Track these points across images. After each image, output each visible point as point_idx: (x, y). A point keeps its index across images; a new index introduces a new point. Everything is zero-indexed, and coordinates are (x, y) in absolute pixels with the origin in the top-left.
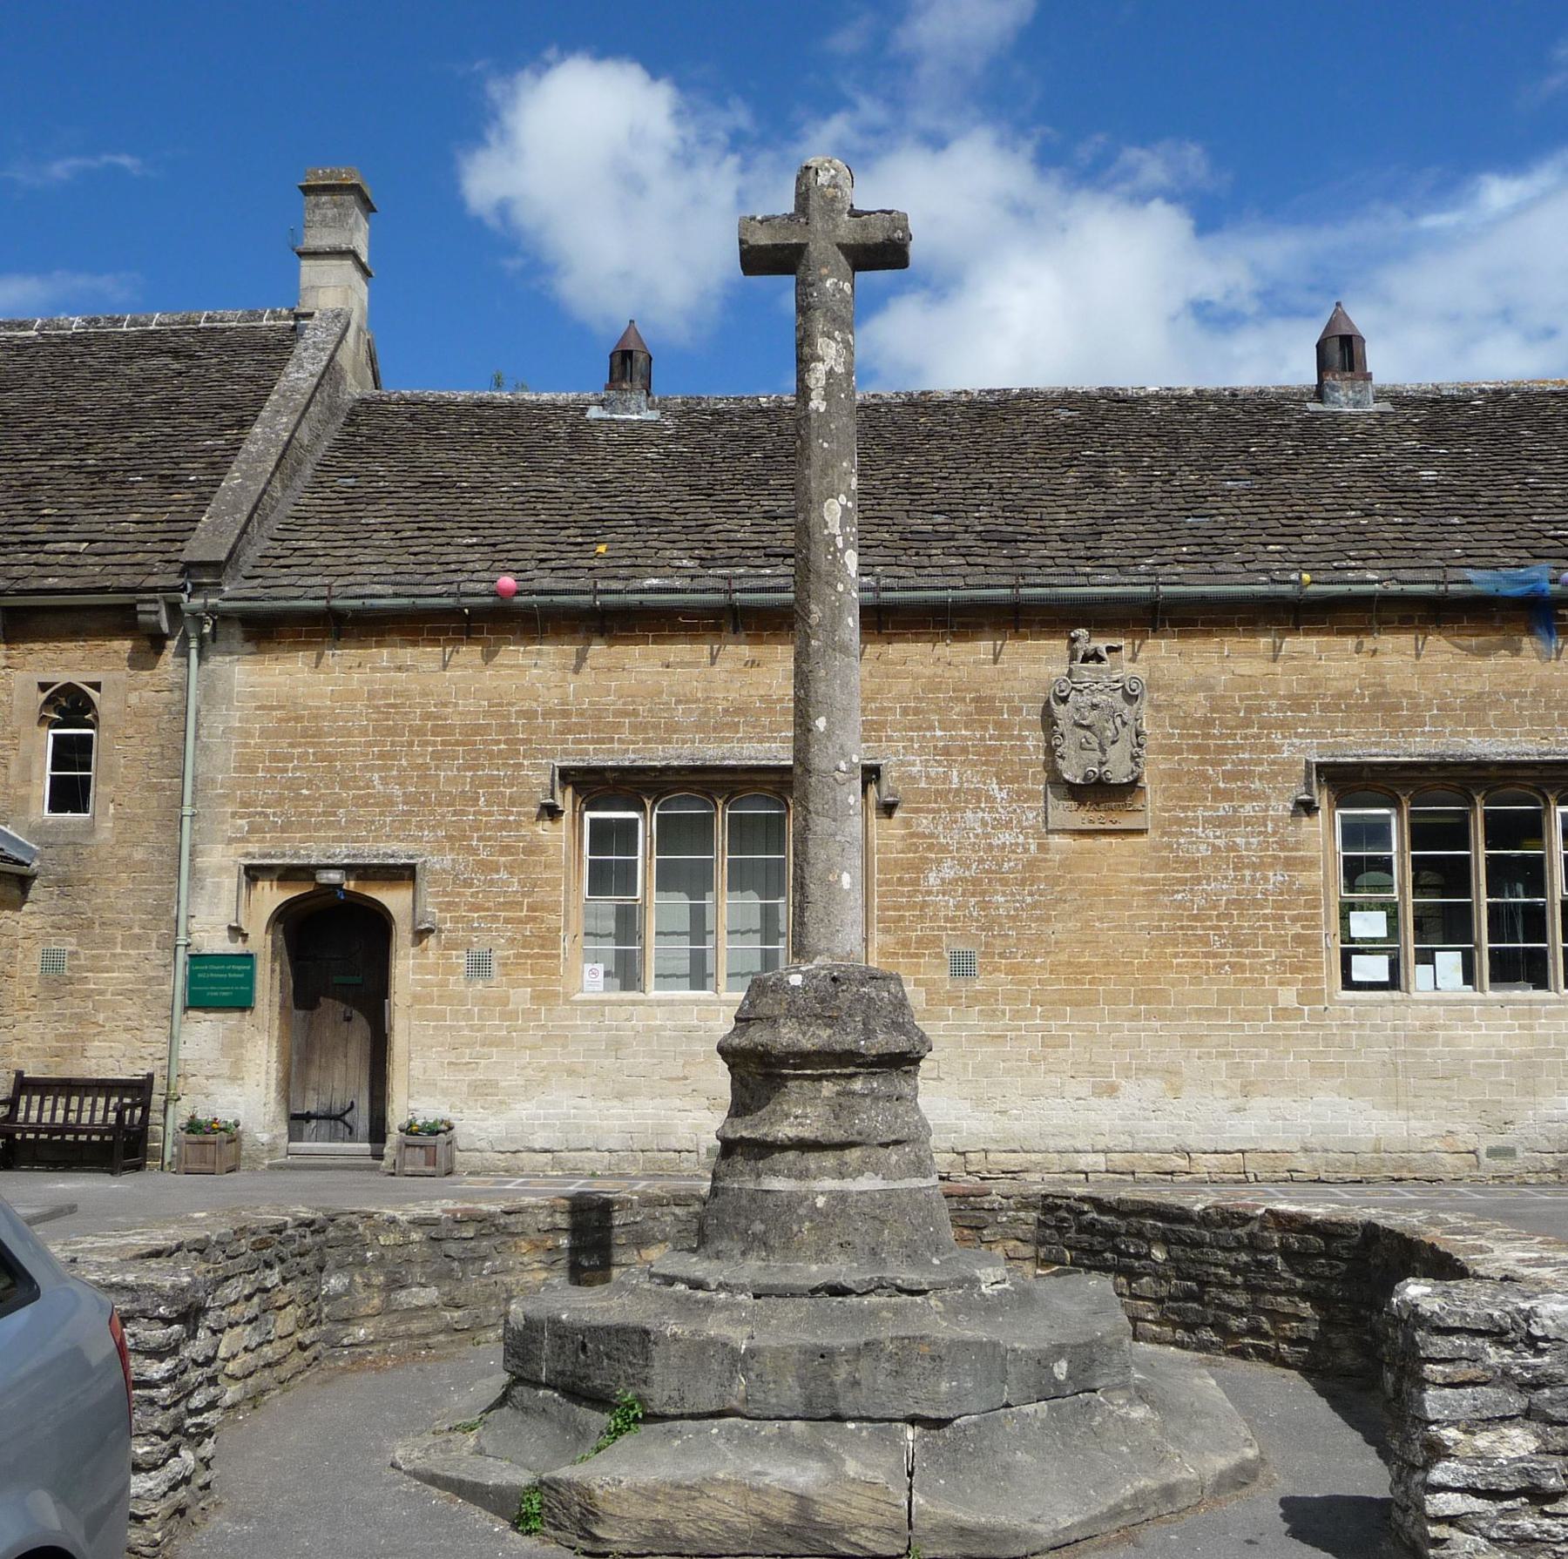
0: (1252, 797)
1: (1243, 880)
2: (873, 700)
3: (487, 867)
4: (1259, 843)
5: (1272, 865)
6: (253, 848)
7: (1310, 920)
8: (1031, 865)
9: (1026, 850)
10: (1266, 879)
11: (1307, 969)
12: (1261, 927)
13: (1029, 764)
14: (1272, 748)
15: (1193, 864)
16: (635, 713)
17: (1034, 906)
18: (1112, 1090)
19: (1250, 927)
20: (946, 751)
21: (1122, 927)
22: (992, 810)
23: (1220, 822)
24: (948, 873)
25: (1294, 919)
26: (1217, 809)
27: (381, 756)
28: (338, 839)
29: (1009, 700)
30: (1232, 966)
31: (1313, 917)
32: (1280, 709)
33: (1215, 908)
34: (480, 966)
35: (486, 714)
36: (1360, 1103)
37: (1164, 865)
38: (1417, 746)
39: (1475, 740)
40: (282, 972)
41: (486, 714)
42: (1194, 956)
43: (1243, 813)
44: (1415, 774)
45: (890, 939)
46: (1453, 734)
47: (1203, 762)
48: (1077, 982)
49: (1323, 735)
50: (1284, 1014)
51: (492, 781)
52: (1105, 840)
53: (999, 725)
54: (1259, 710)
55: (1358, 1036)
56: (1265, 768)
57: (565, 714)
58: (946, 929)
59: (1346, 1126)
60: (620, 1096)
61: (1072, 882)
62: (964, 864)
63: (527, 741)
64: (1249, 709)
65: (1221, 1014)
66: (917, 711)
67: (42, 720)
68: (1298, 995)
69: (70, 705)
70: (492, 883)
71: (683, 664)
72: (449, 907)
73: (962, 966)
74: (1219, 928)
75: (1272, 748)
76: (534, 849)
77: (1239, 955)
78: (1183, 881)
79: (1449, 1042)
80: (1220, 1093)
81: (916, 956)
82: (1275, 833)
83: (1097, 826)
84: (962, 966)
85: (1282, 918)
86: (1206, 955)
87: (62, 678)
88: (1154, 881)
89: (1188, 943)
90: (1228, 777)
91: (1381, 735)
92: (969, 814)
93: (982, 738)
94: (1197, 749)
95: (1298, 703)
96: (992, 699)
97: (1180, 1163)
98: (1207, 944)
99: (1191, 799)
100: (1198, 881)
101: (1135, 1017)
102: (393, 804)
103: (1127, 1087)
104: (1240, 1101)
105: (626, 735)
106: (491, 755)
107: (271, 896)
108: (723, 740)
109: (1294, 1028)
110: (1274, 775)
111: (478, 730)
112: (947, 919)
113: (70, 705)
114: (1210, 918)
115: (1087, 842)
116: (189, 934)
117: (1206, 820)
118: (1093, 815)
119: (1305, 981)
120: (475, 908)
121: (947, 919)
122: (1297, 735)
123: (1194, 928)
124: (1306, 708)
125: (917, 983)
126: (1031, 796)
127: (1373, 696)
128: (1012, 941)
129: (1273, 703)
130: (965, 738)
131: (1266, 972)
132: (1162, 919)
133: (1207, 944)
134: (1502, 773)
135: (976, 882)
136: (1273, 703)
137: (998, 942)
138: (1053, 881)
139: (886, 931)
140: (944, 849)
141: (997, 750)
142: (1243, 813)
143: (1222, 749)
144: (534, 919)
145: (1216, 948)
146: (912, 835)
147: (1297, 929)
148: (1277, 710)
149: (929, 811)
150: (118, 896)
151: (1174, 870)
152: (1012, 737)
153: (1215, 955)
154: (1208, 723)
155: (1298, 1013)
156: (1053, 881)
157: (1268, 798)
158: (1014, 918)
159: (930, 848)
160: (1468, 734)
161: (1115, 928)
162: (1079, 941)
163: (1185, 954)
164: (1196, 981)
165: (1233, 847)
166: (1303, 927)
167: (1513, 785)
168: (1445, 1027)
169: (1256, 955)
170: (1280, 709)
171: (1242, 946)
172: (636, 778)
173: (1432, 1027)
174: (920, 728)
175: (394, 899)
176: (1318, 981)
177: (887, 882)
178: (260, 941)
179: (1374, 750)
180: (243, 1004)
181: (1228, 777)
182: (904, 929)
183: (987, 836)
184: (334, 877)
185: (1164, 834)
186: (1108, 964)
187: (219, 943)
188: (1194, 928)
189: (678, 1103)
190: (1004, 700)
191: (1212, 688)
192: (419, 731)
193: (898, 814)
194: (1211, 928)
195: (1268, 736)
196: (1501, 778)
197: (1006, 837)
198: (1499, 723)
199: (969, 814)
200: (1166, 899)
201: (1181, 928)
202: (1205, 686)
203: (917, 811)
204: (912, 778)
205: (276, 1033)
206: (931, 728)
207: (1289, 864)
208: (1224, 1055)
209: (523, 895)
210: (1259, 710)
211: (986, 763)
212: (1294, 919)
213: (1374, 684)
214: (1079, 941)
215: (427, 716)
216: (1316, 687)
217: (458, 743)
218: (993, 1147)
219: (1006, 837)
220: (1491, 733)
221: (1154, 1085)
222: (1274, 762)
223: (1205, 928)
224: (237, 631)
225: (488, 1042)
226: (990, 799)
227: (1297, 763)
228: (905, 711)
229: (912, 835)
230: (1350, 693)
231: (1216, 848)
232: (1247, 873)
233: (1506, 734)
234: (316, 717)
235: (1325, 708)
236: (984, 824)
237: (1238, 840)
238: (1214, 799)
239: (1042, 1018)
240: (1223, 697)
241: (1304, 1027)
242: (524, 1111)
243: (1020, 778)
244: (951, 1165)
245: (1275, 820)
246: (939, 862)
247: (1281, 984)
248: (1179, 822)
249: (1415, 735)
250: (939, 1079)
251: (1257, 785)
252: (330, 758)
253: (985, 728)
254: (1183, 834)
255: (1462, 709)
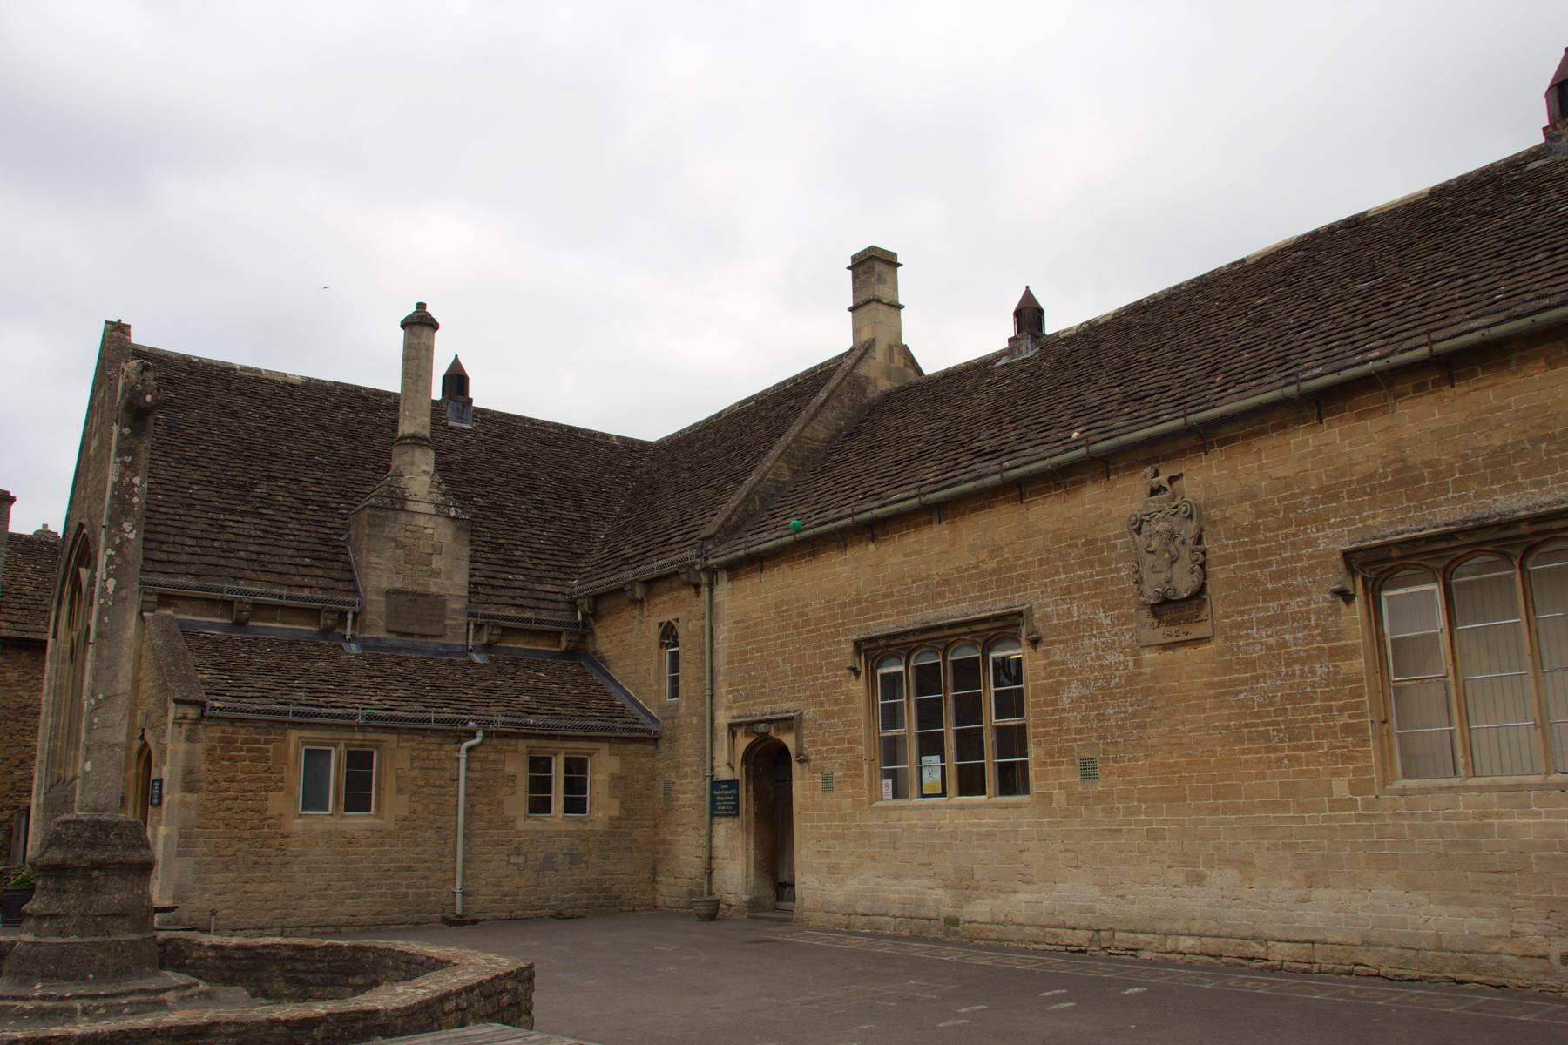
0: (1298, 593)
1: (1293, 675)
2: (1020, 558)
3: (829, 715)
4: (1305, 638)
5: (1318, 658)
6: (735, 712)
7: (1355, 710)
8: (1130, 679)
9: (1126, 667)
10: (1313, 672)
11: (1356, 759)
12: (1313, 720)
13: (1123, 592)
14: (1309, 543)
15: (1250, 664)
16: (891, 595)
17: (1134, 715)
18: (1199, 879)
19: (1303, 720)
20: (1068, 591)
21: (1199, 729)
22: (1102, 635)
23: (1270, 622)
24: (1075, 693)
25: (1342, 709)
26: (1267, 609)
27: (782, 645)
28: (766, 703)
29: (1107, 539)
30: (1290, 759)
31: (1358, 706)
32: (1314, 502)
33: (1271, 704)
34: (827, 785)
35: (825, 609)
36: (1418, 896)
37: (1228, 669)
38: (1445, 513)
39: (1501, 498)
40: (755, 790)
41: (825, 609)
42: (1258, 752)
43: (1289, 610)
44: (1444, 545)
45: (1041, 751)
46: (1478, 495)
47: (1253, 566)
48: (1169, 780)
49: (1353, 522)
50: (1337, 804)
51: (828, 655)
52: (1182, 651)
53: (1102, 562)
54: (1295, 508)
55: (1410, 826)
56: (1305, 563)
57: (859, 601)
58: (1075, 740)
59: (1404, 920)
60: (897, 877)
61: (1160, 691)
62: (1085, 683)
63: (842, 624)
64: (1287, 509)
65: (1284, 806)
66: (1048, 561)
67: (662, 645)
68: (1351, 785)
69: (669, 634)
70: (830, 726)
71: (916, 553)
72: (813, 744)
73: (1088, 770)
74: (1277, 723)
75: (1309, 543)
76: (849, 700)
77: (1296, 748)
78: (1244, 682)
79: (1506, 831)
80: (1287, 883)
81: (1058, 764)
82: (1317, 625)
83: (1175, 639)
84: (1088, 770)
85: (1330, 709)
86: (1268, 750)
87: (666, 618)
88: (1221, 684)
89: (1252, 740)
90: (1275, 577)
91: (1406, 510)
92: (1086, 641)
93: (1091, 576)
94: (1249, 555)
95: (1329, 494)
96: (1095, 541)
97: (1260, 950)
98: (1268, 739)
99: (1246, 603)
100: (1256, 679)
101: (1215, 810)
102: (787, 676)
103: (1212, 875)
104: (1303, 892)
105: (888, 611)
106: (827, 636)
107: (743, 742)
108: (937, 606)
109: (1348, 819)
110: (1312, 569)
111: (820, 620)
112: (1077, 732)
113: (669, 634)
114: (1268, 714)
115: (1169, 654)
116: (712, 769)
117: (1259, 621)
118: (1172, 629)
119: (1356, 771)
120: (824, 744)
121: (1077, 732)
122: (1331, 526)
123: (1255, 725)
124: (1335, 497)
125: (1061, 786)
126: (1127, 619)
127: (1396, 472)
128: (1121, 747)
129: (1306, 499)
130: (1080, 577)
131: (1320, 764)
132: (1230, 719)
133: (1268, 739)
134: (1536, 528)
135: (1093, 698)
136: (1306, 499)
137: (1111, 748)
138: (1147, 692)
139: (1039, 744)
140: (1071, 672)
141: (1101, 583)
142: (1289, 610)
143: (1267, 552)
144: (850, 749)
145: (1274, 743)
146: (1051, 664)
147: (1345, 719)
148: (1311, 505)
149: (1061, 642)
150: (687, 747)
151: (1237, 671)
152: (1111, 571)
153: (1276, 750)
154: (1254, 529)
155: (1351, 804)
156: (1147, 692)
157: (1309, 592)
158: (1120, 727)
159: (1062, 673)
160: (1495, 492)
161: (1194, 730)
162: (1168, 744)
163: (1250, 751)
164: (1261, 775)
165: (1283, 644)
166: (1350, 717)
167: (1556, 539)
168: (1499, 815)
169: (1310, 747)
170: (1314, 502)
171: (1296, 739)
172: (898, 641)
173: (1485, 816)
174: (1051, 575)
175: (789, 740)
176: (1367, 770)
177: (1037, 704)
178: (739, 773)
179: (1401, 528)
180: (734, 811)
181: (1275, 577)
182: (1051, 742)
183: (1099, 658)
184: (762, 728)
185: (1227, 639)
186: (1190, 764)
187: (723, 774)
188: (1255, 725)
189: (926, 882)
190: (1104, 540)
191: (1254, 496)
192: (796, 627)
193: (1041, 648)
194: (1269, 724)
195: (1305, 532)
196: (1534, 534)
197: (1112, 658)
198: (1526, 475)
199: (1086, 641)
200: (1231, 699)
201: (1246, 725)
202: (1248, 495)
203: (1052, 643)
204: (1047, 616)
205: (752, 831)
206: (1058, 573)
207: (1334, 654)
208: (1289, 846)
209: (846, 732)
210: (1295, 508)
211: (1095, 596)
212: (1342, 709)
213: (1396, 461)
214: (1168, 744)
215: (801, 615)
216: (1342, 475)
217: (813, 631)
218: (1117, 926)
219: (1112, 658)
220: (1519, 487)
221: (1233, 875)
222: (1312, 556)
223: (1266, 724)
224: (723, 576)
225: (836, 837)
226: (1100, 626)
227: (1332, 553)
228: (1041, 565)
229: (1051, 664)
230: (1372, 476)
231: (1269, 647)
232: (1297, 667)
233: (1536, 484)
234: (756, 625)
235: (1351, 494)
236: (1097, 648)
237: (1287, 637)
238: (1265, 601)
239: (1146, 813)
240: (1265, 502)
241: (1359, 817)
242: (853, 884)
243: (1120, 604)
244: (1091, 940)
245: (1317, 613)
246: (1070, 683)
247: (1334, 774)
248: (1238, 626)
249: (1439, 505)
250: (1077, 867)
251: (1298, 581)
252: (761, 650)
253: (1092, 566)
254: (1241, 637)
255: (1485, 467)
